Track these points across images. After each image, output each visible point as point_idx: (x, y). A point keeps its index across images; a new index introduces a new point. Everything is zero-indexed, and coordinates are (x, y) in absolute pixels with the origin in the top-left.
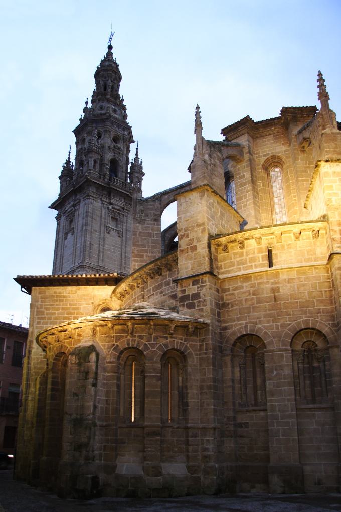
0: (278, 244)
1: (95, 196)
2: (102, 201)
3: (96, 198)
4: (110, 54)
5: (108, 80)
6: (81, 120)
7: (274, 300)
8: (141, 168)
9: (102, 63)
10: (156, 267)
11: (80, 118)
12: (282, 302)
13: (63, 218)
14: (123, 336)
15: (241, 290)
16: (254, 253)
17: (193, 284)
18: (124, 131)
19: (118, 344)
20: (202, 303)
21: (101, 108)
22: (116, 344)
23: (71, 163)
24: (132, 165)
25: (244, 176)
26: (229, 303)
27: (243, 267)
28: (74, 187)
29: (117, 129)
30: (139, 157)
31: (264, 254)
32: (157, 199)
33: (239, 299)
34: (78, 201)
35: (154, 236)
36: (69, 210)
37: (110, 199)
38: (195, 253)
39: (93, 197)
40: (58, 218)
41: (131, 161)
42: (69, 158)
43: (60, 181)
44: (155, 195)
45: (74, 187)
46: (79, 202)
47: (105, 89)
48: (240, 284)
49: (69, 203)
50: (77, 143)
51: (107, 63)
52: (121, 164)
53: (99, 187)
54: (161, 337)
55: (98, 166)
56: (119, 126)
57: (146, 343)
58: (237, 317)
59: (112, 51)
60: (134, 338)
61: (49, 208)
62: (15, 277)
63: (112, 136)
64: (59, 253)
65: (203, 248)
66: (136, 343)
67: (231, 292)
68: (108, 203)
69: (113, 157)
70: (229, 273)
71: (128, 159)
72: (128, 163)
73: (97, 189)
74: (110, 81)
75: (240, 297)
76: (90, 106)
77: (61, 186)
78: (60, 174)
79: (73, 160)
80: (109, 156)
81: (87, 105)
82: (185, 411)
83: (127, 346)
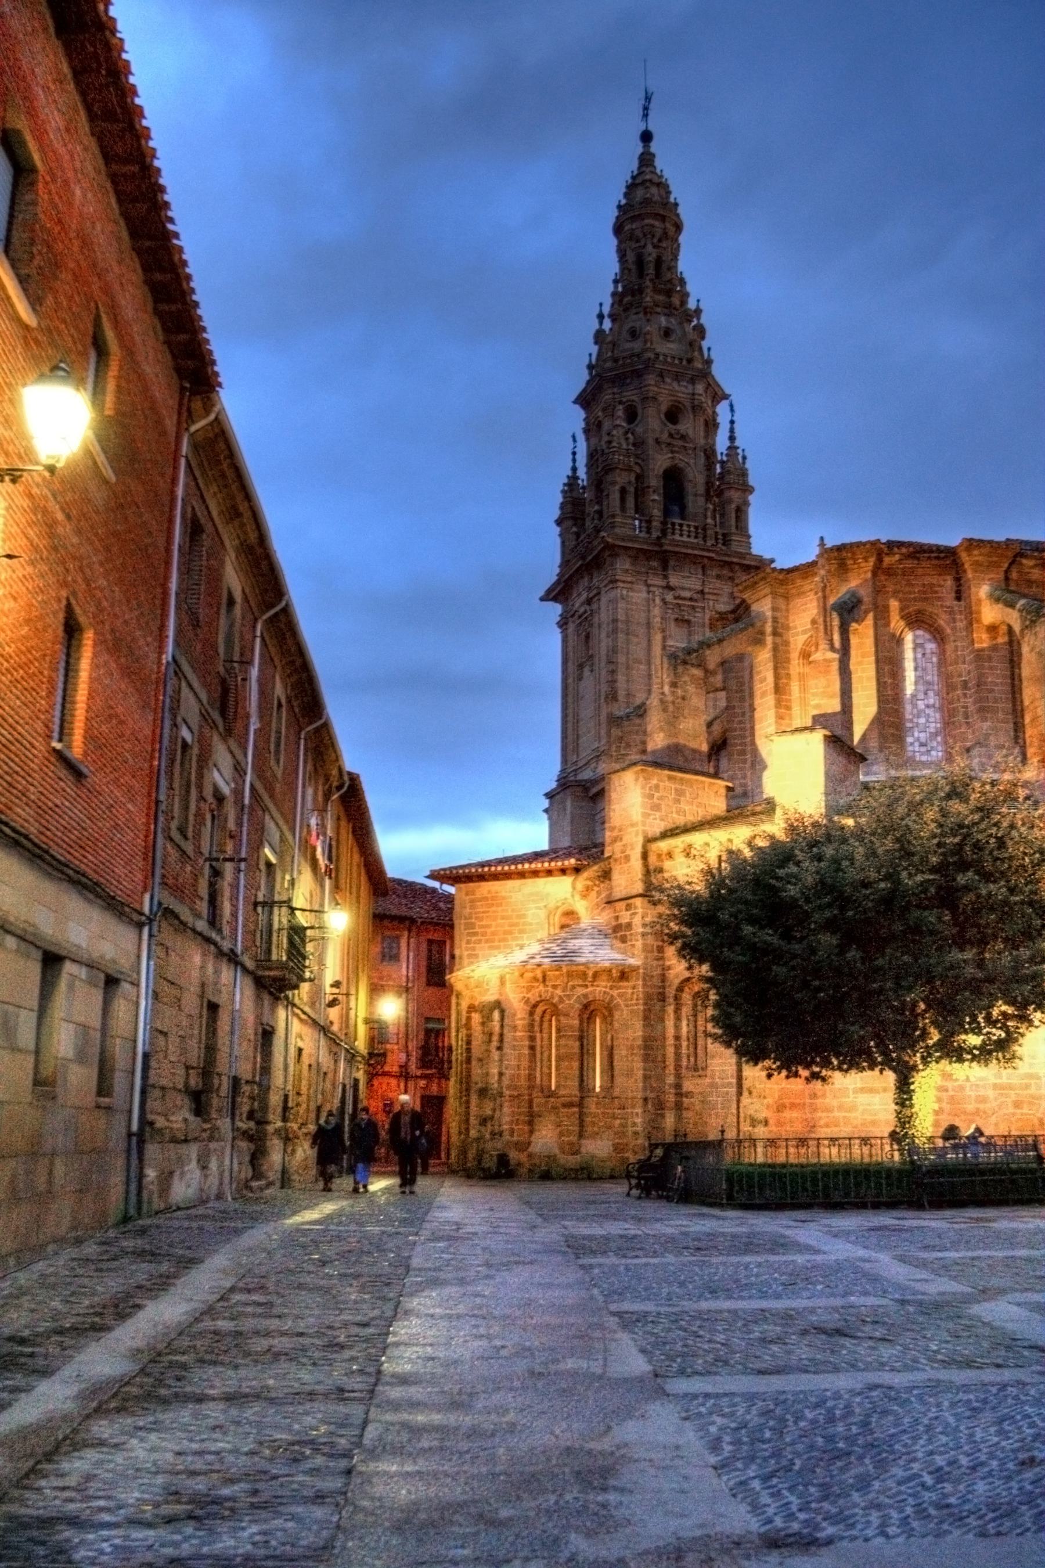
2: (649, 586)
3: (631, 583)
4: (646, 160)
5: (644, 247)
6: (590, 367)
9: (631, 188)
11: (587, 362)
13: (571, 627)
18: (693, 384)
21: (634, 334)
24: (722, 467)
25: (765, 679)
28: (583, 558)
30: (737, 443)
36: (582, 610)
37: (665, 577)
40: (563, 624)
42: (574, 469)
45: (583, 558)
46: (599, 593)
47: (641, 274)
49: (579, 595)
50: (587, 431)
51: (640, 193)
52: (691, 476)
53: (639, 555)
56: (677, 377)
59: (654, 147)
61: (542, 599)
62: (428, 873)
63: (664, 408)
64: (570, 711)
68: (663, 588)
74: (650, 248)
77: (563, 543)
78: (556, 513)
79: (582, 473)
80: (660, 461)
81: (601, 323)
82: (612, 1076)
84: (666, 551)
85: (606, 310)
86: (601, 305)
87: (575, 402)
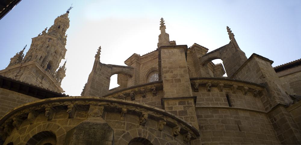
0: (233, 94)
1: (34, 75)
2: (37, 79)
3: (34, 76)
7: (238, 129)
8: (65, 72)
9: (62, 16)
10: (132, 92)
12: (245, 132)
14: (135, 125)
15: (212, 118)
16: (218, 96)
17: (180, 104)
19: (129, 131)
20: (190, 119)
22: (127, 131)
23: (23, 55)
26: (203, 126)
27: (211, 103)
29: (59, 47)
30: (65, 66)
31: (225, 98)
32: (110, 67)
33: (211, 124)
34: (21, 74)
35: (104, 87)
38: (179, 83)
39: (32, 75)
41: (60, 67)
42: (23, 51)
43: (10, 61)
44: (109, 65)
45: (21, 65)
46: (22, 75)
48: (210, 114)
54: (168, 136)
55: (42, 60)
57: (157, 137)
58: (212, 138)
60: (145, 130)
63: (55, 49)
65: (187, 82)
66: (148, 136)
67: (203, 118)
69: (52, 60)
70: (200, 105)
71: (59, 65)
72: (57, 67)
73: (37, 71)
74: (63, 25)
75: (212, 123)
76: (47, 32)
79: (25, 53)
80: (50, 58)
83: (138, 136)
84: (45, 74)
85: (48, 29)
86: (47, 28)
87: (32, 39)
